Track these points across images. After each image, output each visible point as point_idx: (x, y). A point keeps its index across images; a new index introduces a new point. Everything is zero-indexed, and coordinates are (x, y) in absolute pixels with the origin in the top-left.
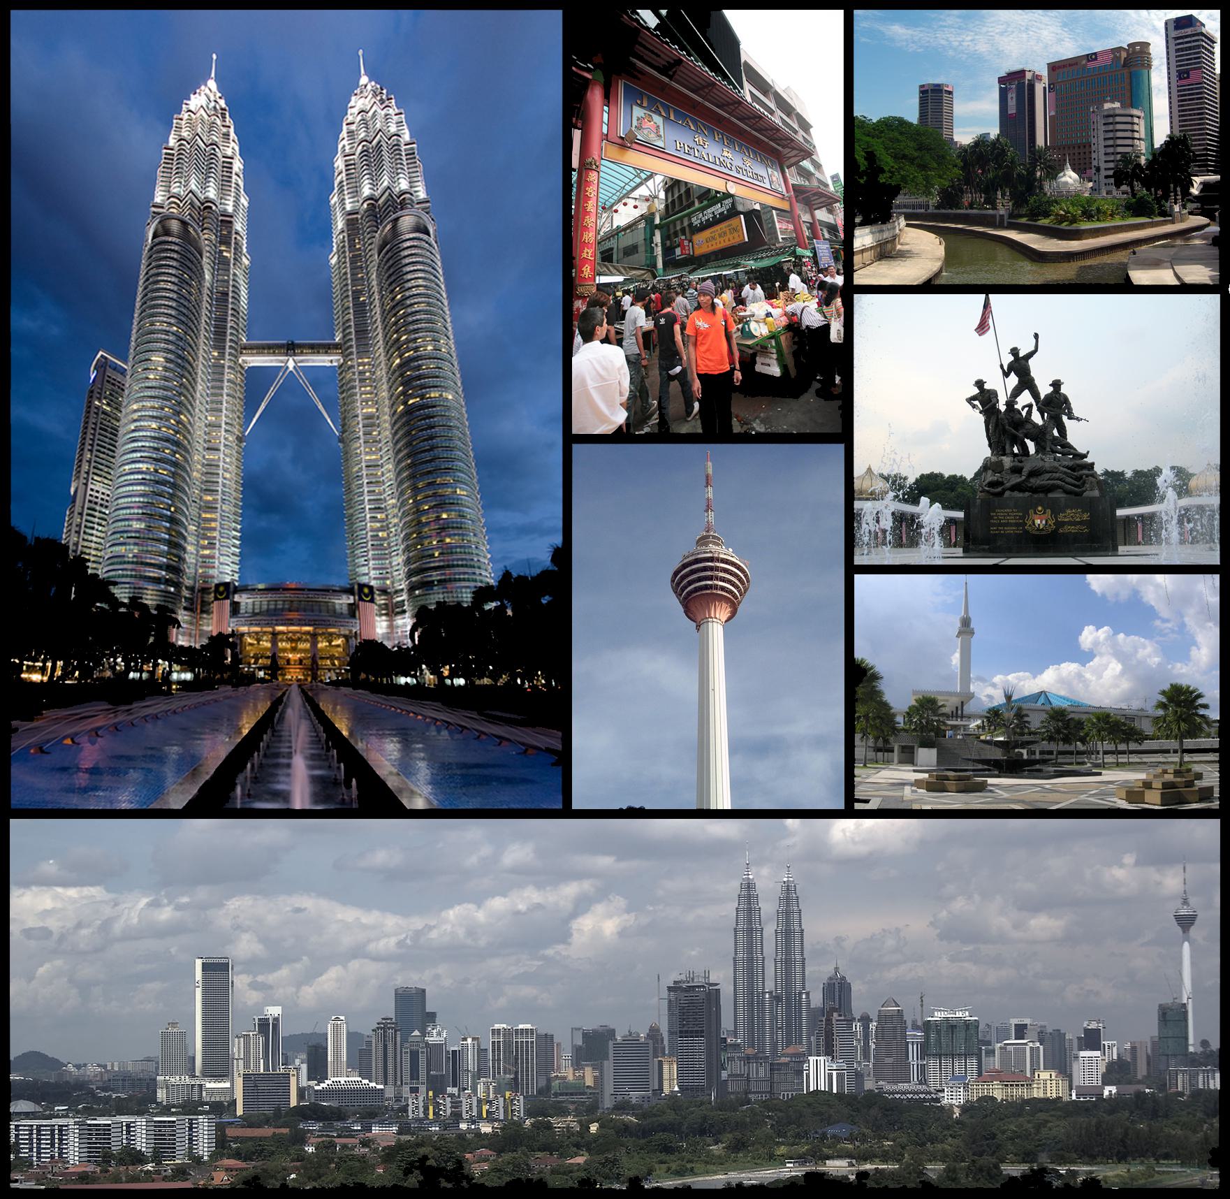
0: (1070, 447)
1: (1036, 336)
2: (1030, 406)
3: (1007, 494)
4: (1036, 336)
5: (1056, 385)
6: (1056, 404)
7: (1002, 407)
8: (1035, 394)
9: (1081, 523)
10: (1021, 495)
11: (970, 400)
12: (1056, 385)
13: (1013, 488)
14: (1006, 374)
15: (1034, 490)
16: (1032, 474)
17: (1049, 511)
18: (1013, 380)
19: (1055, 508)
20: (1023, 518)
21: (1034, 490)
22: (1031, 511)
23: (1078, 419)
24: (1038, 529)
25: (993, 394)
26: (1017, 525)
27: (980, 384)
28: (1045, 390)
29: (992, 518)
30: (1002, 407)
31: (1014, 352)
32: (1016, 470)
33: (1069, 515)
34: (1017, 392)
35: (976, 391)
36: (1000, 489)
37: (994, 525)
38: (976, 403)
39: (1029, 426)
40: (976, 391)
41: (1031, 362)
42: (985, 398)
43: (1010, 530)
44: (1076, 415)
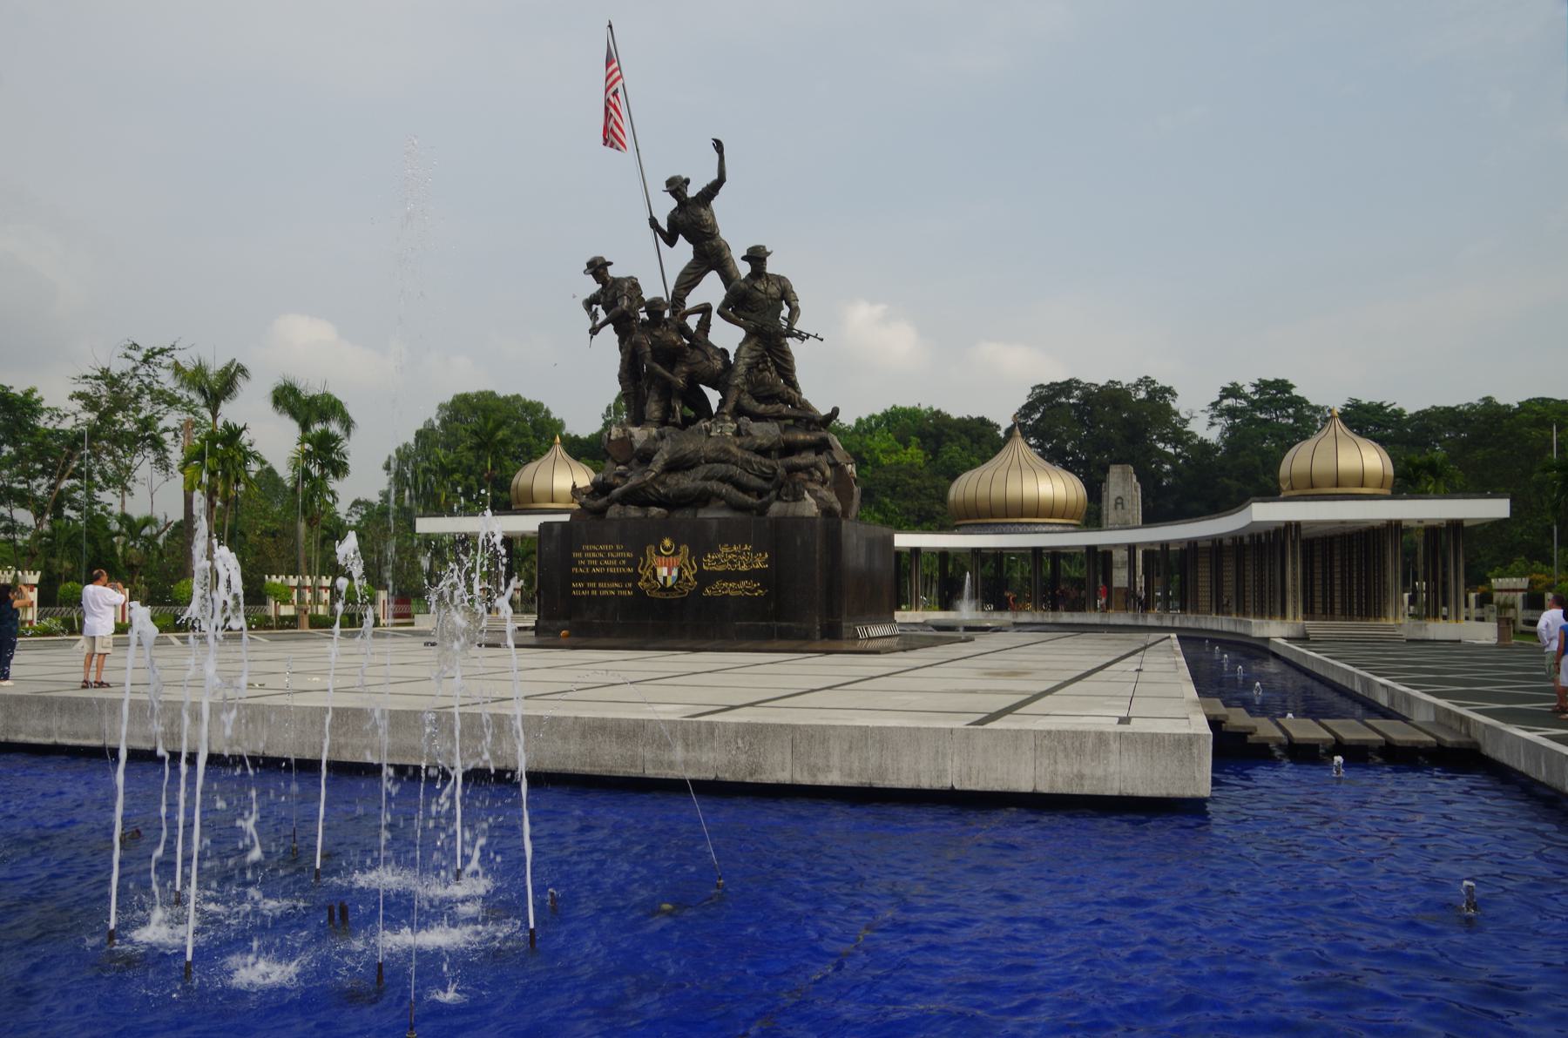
1: (718, 146)
2: (705, 310)
3: (614, 511)
4: (718, 146)
5: (756, 257)
9: (750, 575)
11: (589, 304)
13: (629, 498)
14: (671, 242)
17: (685, 549)
18: (683, 252)
19: (700, 544)
20: (633, 563)
22: (650, 549)
23: (802, 336)
24: (664, 588)
26: (621, 578)
27: (597, 268)
29: (575, 562)
31: (676, 186)
32: (645, 457)
33: (724, 557)
34: (689, 280)
35: (592, 287)
36: (602, 501)
37: (579, 578)
40: (592, 287)
41: (715, 204)
42: (613, 299)
43: (609, 589)
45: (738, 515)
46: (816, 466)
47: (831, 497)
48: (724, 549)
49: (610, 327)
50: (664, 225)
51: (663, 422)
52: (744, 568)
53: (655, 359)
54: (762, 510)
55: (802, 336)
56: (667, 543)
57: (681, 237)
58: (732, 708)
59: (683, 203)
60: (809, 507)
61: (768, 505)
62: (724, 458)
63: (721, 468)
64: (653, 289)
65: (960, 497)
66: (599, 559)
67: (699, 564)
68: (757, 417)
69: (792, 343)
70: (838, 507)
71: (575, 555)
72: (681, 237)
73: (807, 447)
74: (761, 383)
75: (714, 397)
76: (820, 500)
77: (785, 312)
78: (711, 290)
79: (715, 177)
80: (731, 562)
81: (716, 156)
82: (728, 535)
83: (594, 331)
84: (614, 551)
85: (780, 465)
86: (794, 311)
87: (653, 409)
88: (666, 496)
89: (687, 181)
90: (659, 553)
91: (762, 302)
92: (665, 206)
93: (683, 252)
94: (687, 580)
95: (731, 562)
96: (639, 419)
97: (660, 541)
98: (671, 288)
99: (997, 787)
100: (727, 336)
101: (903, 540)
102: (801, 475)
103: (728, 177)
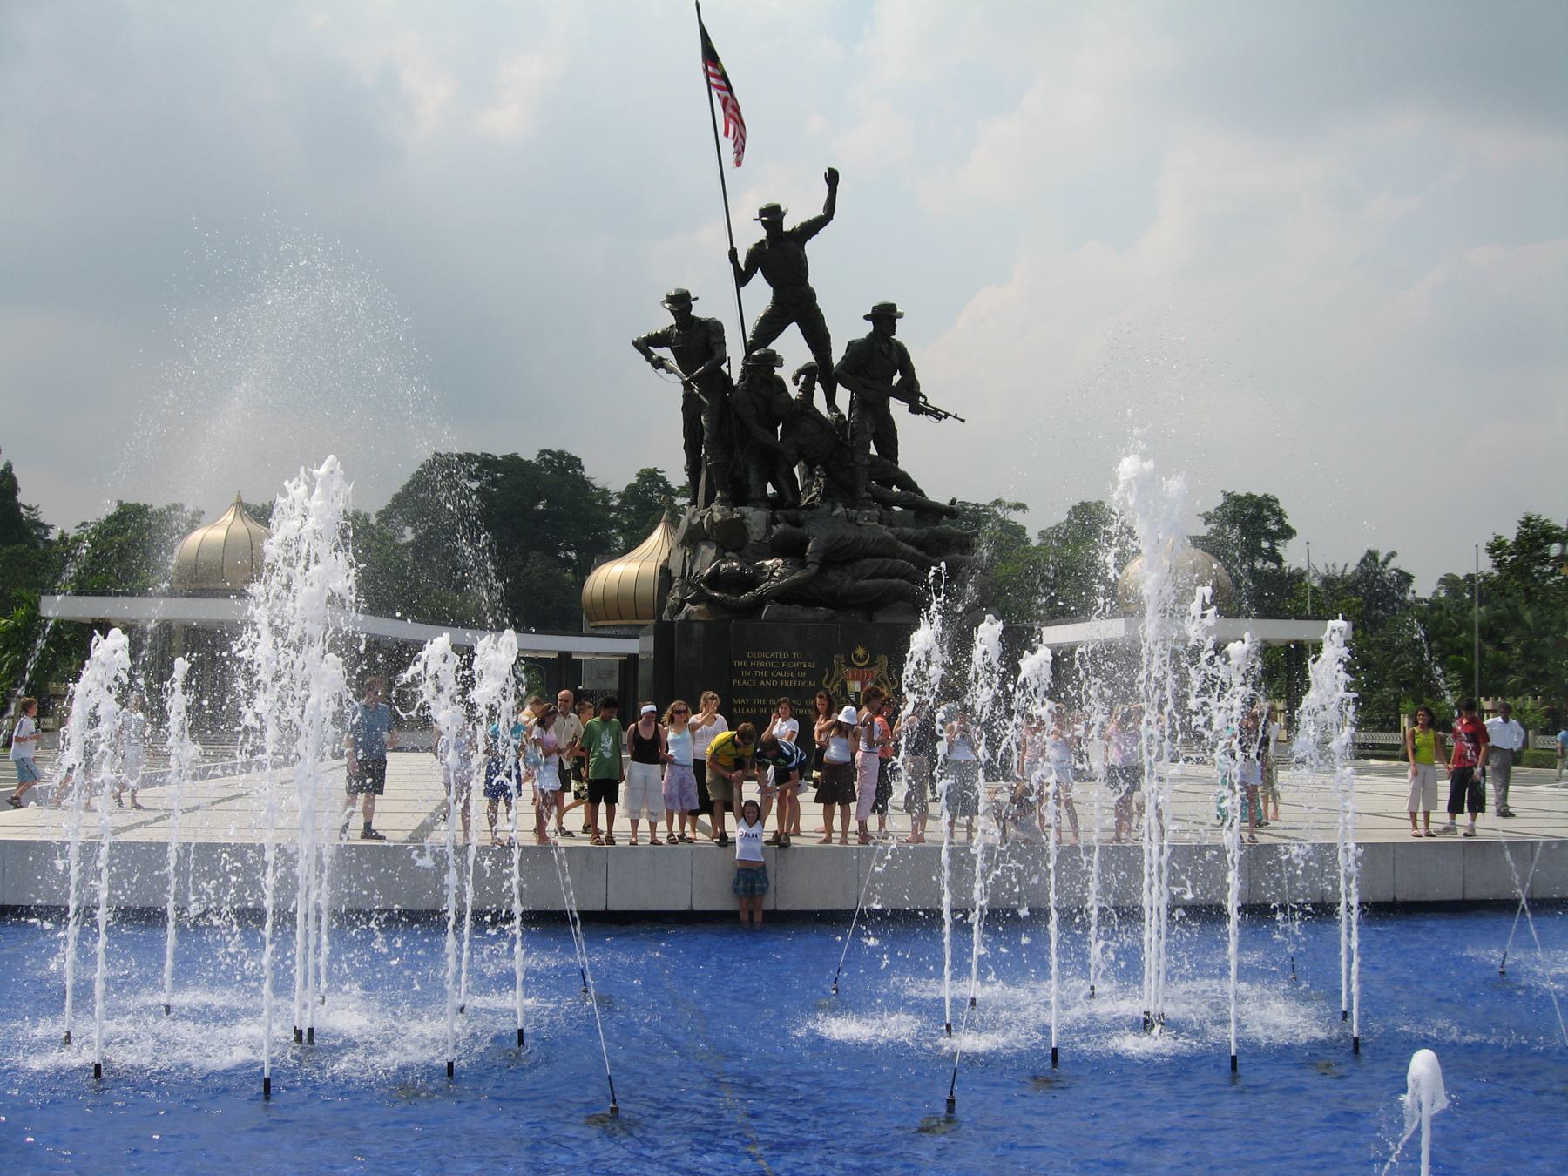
0: (906, 482)
1: (832, 178)
4: (832, 178)
5: (884, 317)
6: (881, 365)
7: (735, 368)
8: (817, 337)
10: (809, 614)
11: (645, 345)
12: (884, 317)
14: (742, 278)
15: (839, 603)
16: (836, 557)
18: (760, 294)
20: (816, 675)
21: (839, 603)
22: (837, 659)
23: (937, 414)
25: (711, 333)
27: (680, 302)
28: (847, 328)
30: (735, 368)
31: (772, 216)
34: (770, 327)
35: (665, 320)
38: (665, 353)
40: (665, 320)
41: (812, 248)
44: (933, 402)
50: (742, 260)
56: (860, 651)
57: (758, 277)
65: (598, 592)
66: (770, 670)
72: (758, 277)
79: (820, 212)
81: (825, 189)
84: (791, 659)
90: (850, 664)
92: (752, 234)
97: (852, 649)
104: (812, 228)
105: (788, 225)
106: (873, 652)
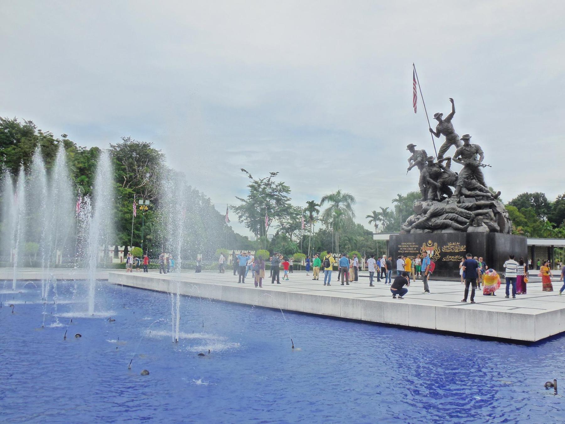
1: (452, 101)
2: (449, 159)
3: (412, 231)
4: (452, 101)
5: (466, 138)
13: (417, 227)
14: (438, 135)
17: (436, 244)
18: (442, 140)
19: (441, 242)
23: (484, 166)
27: (411, 148)
29: (399, 249)
31: (438, 116)
34: (444, 149)
36: (410, 227)
39: (446, 176)
40: (410, 154)
41: (453, 121)
45: (456, 232)
46: (487, 213)
47: (496, 225)
48: (450, 244)
49: (416, 167)
51: (434, 199)
52: (457, 251)
53: (431, 177)
54: (465, 230)
55: (484, 166)
56: (430, 242)
58: (518, 308)
59: (441, 122)
60: (484, 229)
61: (467, 227)
62: (453, 211)
63: (451, 215)
64: (432, 153)
66: (407, 248)
67: (441, 249)
68: (467, 196)
69: (481, 168)
70: (498, 228)
71: (399, 246)
73: (485, 206)
74: (470, 184)
75: (453, 189)
76: (489, 226)
77: (478, 156)
78: (452, 151)
80: (452, 249)
82: (451, 238)
83: (409, 169)
84: (412, 245)
85: (472, 213)
86: (482, 158)
87: (430, 195)
88: (431, 225)
89: (442, 114)
91: (469, 154)
92: (435, 124)
93: (442, 140)
94: (437, 255)
95: (452, 249)
96: (425, 199)
98: (438, 152)
99: (378, 322)
100: (457, 168)
101: (531, 242)
102: (480, 217)
103: (456, 111)
104: (451, 116)
105: (443, 118)
106: (433, 242)
